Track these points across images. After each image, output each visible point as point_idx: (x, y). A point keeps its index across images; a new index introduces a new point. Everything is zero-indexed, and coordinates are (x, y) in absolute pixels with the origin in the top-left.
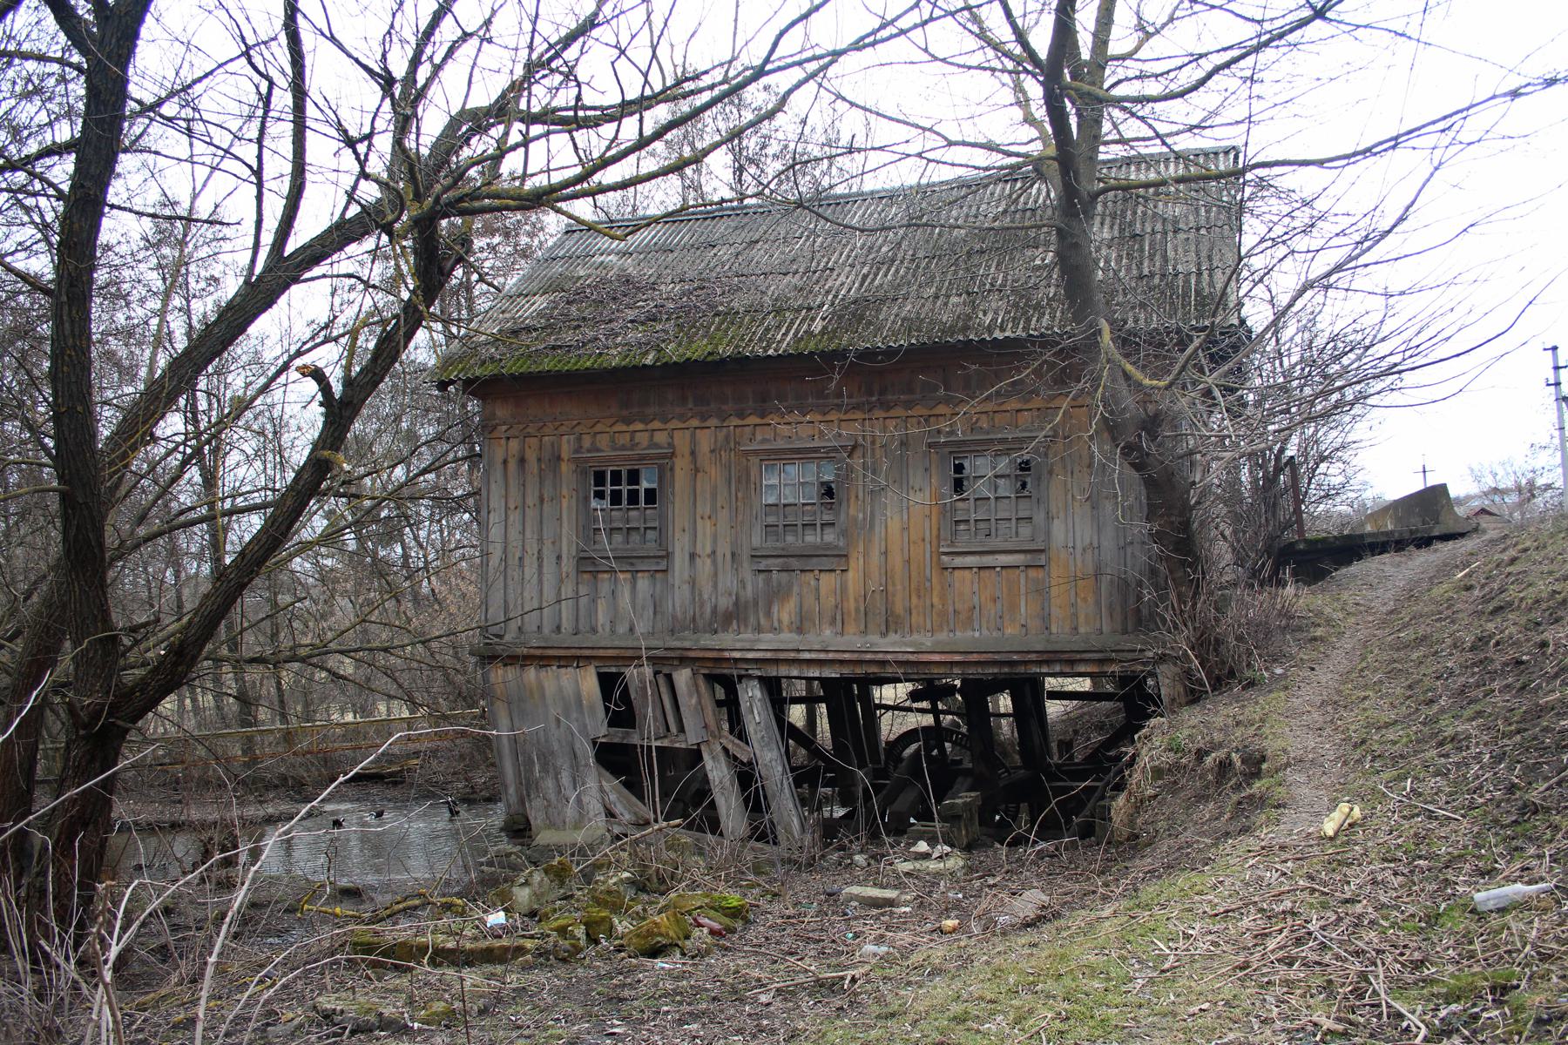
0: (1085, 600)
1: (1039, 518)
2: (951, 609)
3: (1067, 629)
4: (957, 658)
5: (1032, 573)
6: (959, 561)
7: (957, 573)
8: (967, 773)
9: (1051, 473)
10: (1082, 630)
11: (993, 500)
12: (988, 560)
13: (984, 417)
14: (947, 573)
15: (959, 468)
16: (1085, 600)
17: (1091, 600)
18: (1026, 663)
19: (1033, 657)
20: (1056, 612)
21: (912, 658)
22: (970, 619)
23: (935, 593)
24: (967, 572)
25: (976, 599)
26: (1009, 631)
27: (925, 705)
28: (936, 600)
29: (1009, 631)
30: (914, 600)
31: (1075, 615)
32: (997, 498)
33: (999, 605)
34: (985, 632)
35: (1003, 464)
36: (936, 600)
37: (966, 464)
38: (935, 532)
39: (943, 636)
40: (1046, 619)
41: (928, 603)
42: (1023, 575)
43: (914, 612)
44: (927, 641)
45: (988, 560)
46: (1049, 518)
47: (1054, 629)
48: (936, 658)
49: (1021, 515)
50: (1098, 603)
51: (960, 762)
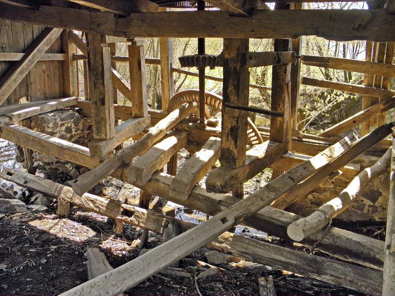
27: (194, 70)
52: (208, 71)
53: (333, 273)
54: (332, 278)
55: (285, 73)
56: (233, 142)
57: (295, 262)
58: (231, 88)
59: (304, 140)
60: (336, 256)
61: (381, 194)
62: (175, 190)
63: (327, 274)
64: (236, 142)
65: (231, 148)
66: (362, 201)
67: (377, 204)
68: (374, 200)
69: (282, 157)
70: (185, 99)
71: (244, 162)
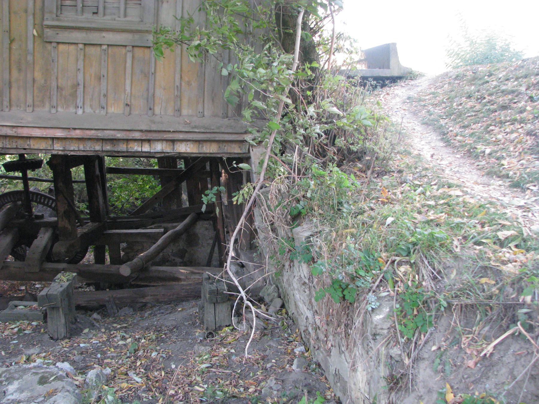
0: (189, 83)
2: (54, 84)
3: (170, 111)
4: (59, 134)
5: (138, 52)
6: (64, 36)
7: (61, 47)
8: (48, 225)
10: (185, 112)
16: (189, 83)
17: (194, 84)
18: (128, 140)
19: (137, 135)
20: (159, 93)
21: (10, 132)
22: (74, 95)
23: (37, 68)
24: (72, 47)
25: (80, 77)
26: (112, 110)
27: (18, 174)
28: (38, 75)
29: (112, 110)
30: (15, 73)
31: (179, 97)
33: (104, 82)
34: (88, 110)
36: (38, 75)
39: (44, 111)
40: (150, 101)
41: (29, 76)
42: (129, 55)
43: (14, 85)
44: (28, 118)
45: (94, 37)
47: (157, 110)
48: (37, 133)
50: (202, 88)
51: (42, 217)
52: (30, 174)
53: (153, 294)
54: (152, 297)
55: (94, 167)
56: (67, 221)
57: (126, 295)
58: (60, 184)
59: (119, 220)
60: (152, 284)
61: (186, 251)
62: (29, 265)
63: (148, 296)
64: (69, 221)
65: (66, 226)
66: (174, 260)
67: (185, 259)
68: (182, 257)
69: (104, 234)
70: (9, 200)
71: (77, 236)
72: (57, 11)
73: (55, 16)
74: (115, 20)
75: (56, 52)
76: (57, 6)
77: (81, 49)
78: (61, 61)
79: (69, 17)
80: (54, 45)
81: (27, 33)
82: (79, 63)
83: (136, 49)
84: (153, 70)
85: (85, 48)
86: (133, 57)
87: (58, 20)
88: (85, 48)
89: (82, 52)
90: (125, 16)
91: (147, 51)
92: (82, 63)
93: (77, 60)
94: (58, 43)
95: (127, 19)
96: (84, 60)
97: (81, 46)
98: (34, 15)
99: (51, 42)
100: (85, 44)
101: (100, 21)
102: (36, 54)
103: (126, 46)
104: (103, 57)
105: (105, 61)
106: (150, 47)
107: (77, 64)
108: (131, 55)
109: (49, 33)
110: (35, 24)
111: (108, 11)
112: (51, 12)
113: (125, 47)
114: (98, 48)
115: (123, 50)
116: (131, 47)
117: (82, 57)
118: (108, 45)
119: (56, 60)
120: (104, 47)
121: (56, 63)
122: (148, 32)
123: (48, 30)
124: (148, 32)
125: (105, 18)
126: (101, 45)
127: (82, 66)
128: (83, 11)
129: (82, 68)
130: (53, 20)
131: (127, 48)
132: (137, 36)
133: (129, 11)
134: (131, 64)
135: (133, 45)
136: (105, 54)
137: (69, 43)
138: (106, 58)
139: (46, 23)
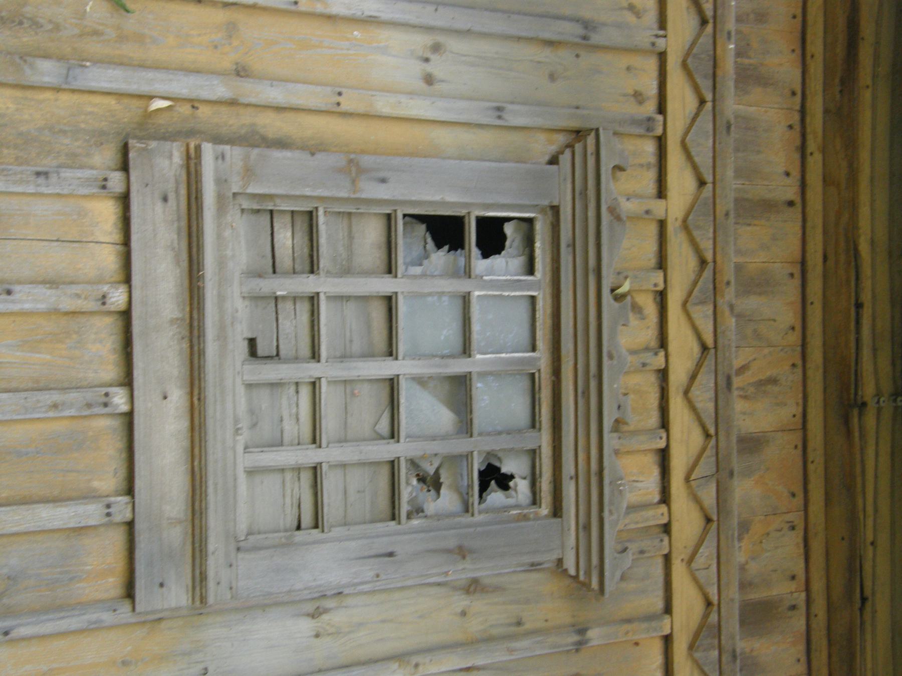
1: (324, 562)
6: (157, 226)
7: (106, 212)
9: (473, 587)
11: (386, 368)
12: (160, 355)
13: (647, 334)
14: (104, 157)
15: (492, 238)
24: (108, 259)
32: (392, 384)
35: (501, 405)
37: (504, 266)
38: (273, 125)
42: (92, 513)
45: (160, 355)
46: (318, 603)
49: (331, 483)
72: (254, 196)
73: (235, 189)
74: (237, 431)
75: (85, 191)
76: (271, 197)
77: (103, 299)
78: (43, 208)
79: (231, 244)
80: (116, 180)
81: (157, 67)
82: (41, 291)
83: (118, 538)
84: (24, 631)
85: (109, 313)
86: (80, 530)
87: (221, 199)
88: (109, 313)
89: (92, 305)
90: (251, 472)
91: (113, 585)
92: (42, 306)
93: (52, 283)
94: (125, 200)
95: (242, 477)
96: (54, 312)
97: (118, 298)
98: (233, 103)
99: (125, 167)
100: (126, 315)
101: (227, 367)
102: (65, 98)
103: (130, 491)
104: (73, 396)
105: (55, 406)
106: (130, 592)
107: (33, 282)
108: (92, 522)
109: (168, 163)
110: (194, 103)
111: (264, 398)
112: (249, 173)
113: (123, 485)
114: (110, 371)
115: (108, 480)
116: (128, 516)
117: (67, 304)
118: (129, 418)
119: (44, 190)
120: (120, 400)
121: (31, 189)
122: (199, 580)
123: (178, 158)
124: (199, 580)
125: (241, 390)
126: (128, 381)
127: (27, 306)
128: (256, 298)
129: (16, 307)
130: (221, 181)
131: (125, 499)
132: (176, 536)
133: (271, 482)
134: (57, 524)
135: (139, 526)
136: (89, 405)
137: (126, 242)
138: (73, 412)
139: (208, 151)
